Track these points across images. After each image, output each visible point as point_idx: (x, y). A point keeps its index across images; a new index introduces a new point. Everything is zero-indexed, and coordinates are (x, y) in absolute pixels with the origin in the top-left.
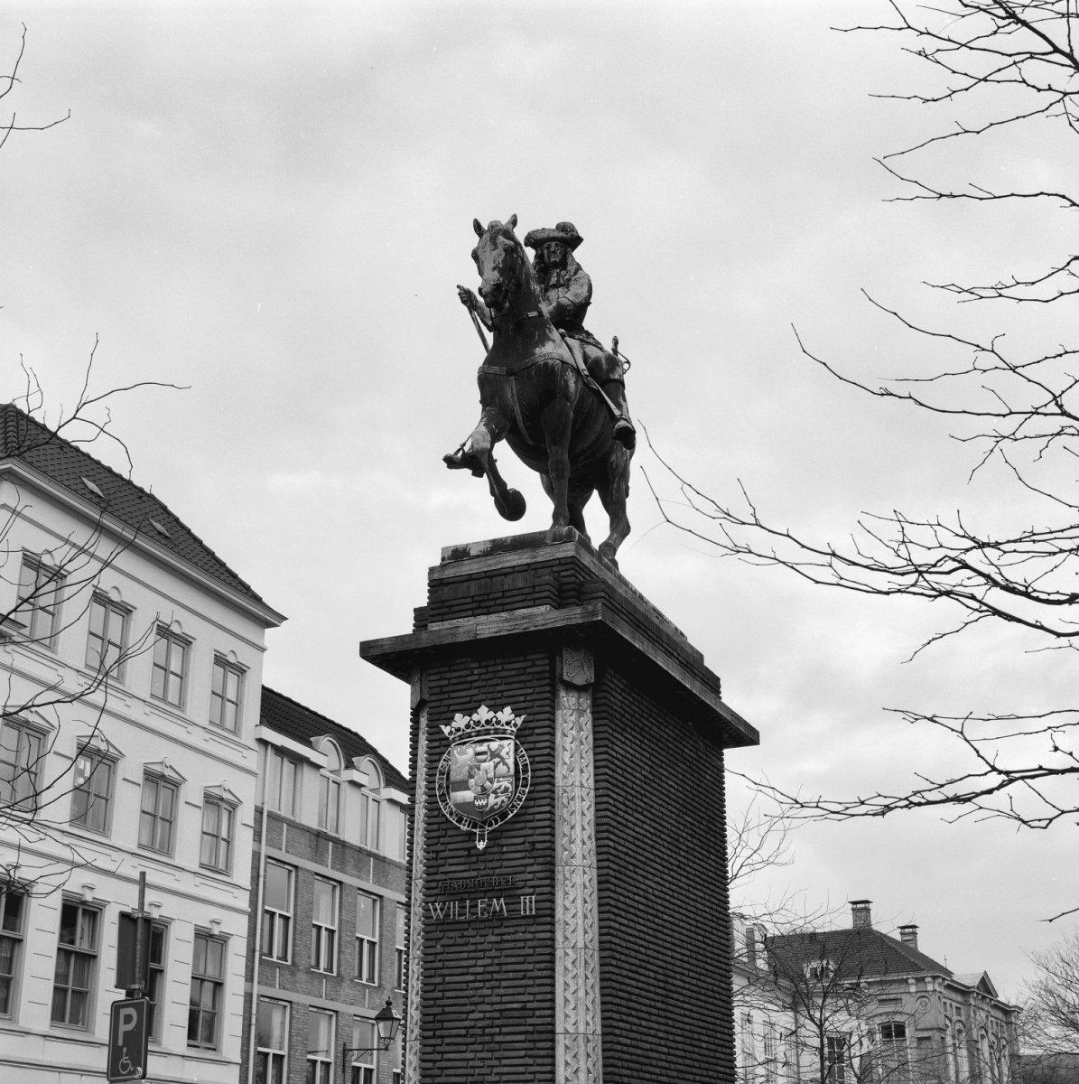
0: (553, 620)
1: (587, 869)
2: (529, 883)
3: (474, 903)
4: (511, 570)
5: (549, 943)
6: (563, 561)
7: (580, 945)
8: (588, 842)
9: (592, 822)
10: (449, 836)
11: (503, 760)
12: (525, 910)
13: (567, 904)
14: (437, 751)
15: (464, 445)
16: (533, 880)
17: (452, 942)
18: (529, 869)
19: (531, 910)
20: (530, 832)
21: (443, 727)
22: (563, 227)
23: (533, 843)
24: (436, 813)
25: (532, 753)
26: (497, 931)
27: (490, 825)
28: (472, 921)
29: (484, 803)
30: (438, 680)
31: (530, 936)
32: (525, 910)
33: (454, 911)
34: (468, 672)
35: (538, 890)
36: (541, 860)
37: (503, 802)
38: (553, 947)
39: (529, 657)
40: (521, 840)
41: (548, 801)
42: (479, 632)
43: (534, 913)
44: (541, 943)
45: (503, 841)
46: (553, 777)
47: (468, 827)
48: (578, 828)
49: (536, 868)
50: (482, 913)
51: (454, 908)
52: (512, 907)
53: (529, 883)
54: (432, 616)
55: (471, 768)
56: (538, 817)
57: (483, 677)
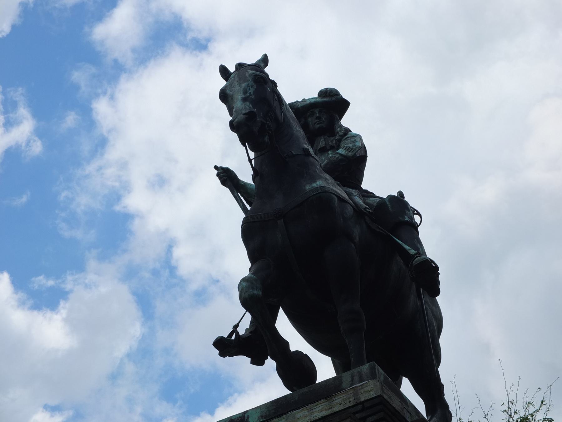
15: (237, 326)
22: (325, 93)
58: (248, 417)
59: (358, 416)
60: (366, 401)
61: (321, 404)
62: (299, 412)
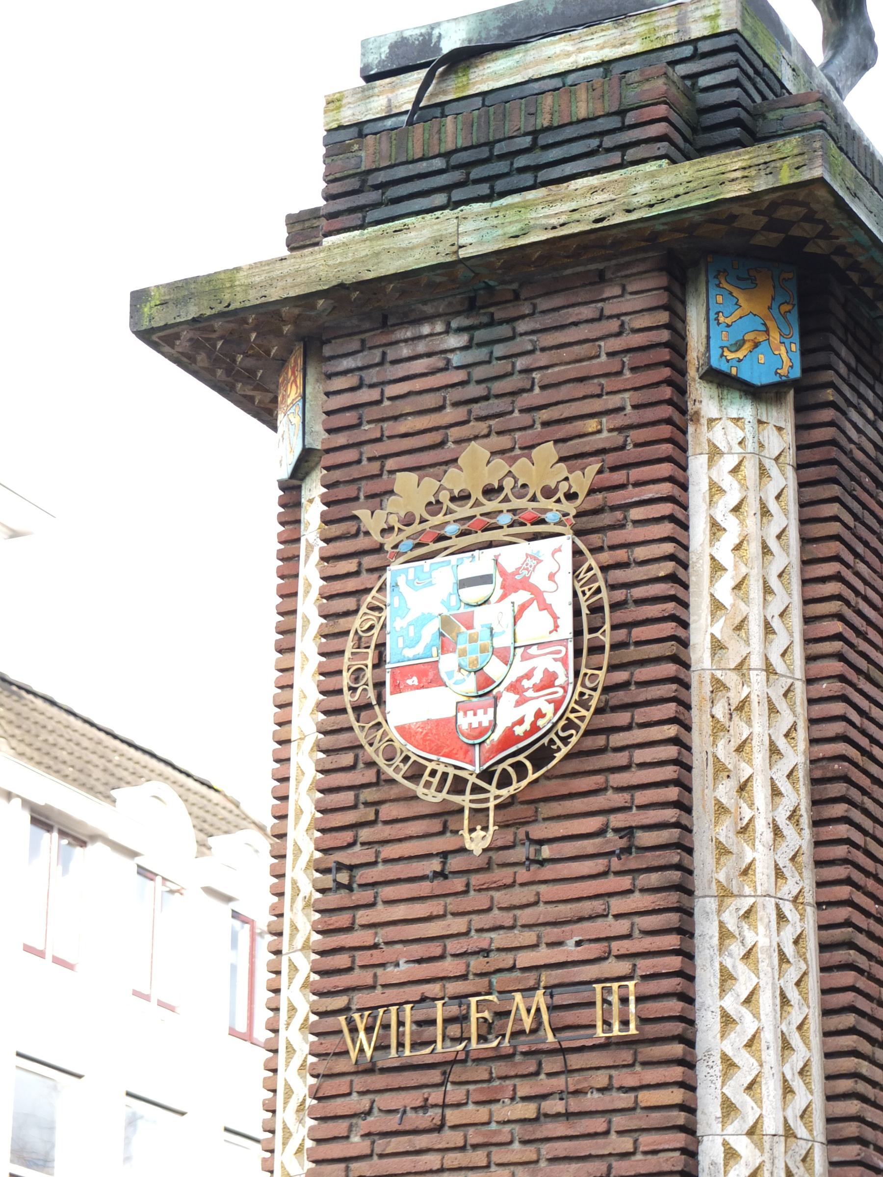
0: (681, 190)
1: (788, 909)
2: (618, 947)
3: (454, 1010)
4: (557, 82)
5: (680, 1118)
6: (704, 47)
7: (772, 1125)
8: (788, 830)
9: (801, 774)
10: (386, 823)
11: (538, 595)
12: (607, 1023)
13: (731, 1003)
14: (351, 585)
16: (629, 936)
17: (392, 1123)
18: (618, 905)
19: (625, 1023)
20: (619, 799)
21: (363, 513)
23: (628, 832)
24: (347, 759)
25: (619, 576)
26: (525, 1088)
27: (505, 782)
28: (454, 1062)
29: (484, 718)
30: (352, 389)
31: (624, 1100)
32: (607, 1023)
33: (401, 1035)
34: (436, 362)
35: (645, 966)
36: (654, 879)
37: (539, 714)
38: (689, 1130)
39: (610, 308)
40: (593, 824)
41: (670, 709)
42: (462, 241)
43: (633, 1030)
44: (656, 1118)
45: (538, 831)
46: (685, 644)
47: (439, 789)
48: (760, 792)
49: (638, 901)
50: (482, 1038)
51: (401, 1024)
52: (570, 1017)
53: (618, 947)
54: (331, 216)
55: (446, 622)
56: (640, 756)
57: (479, 373)
58: (440, 37)
59: (683, 69)
60: (704, 38)
61: (602, 30)
62: (553, 43)
